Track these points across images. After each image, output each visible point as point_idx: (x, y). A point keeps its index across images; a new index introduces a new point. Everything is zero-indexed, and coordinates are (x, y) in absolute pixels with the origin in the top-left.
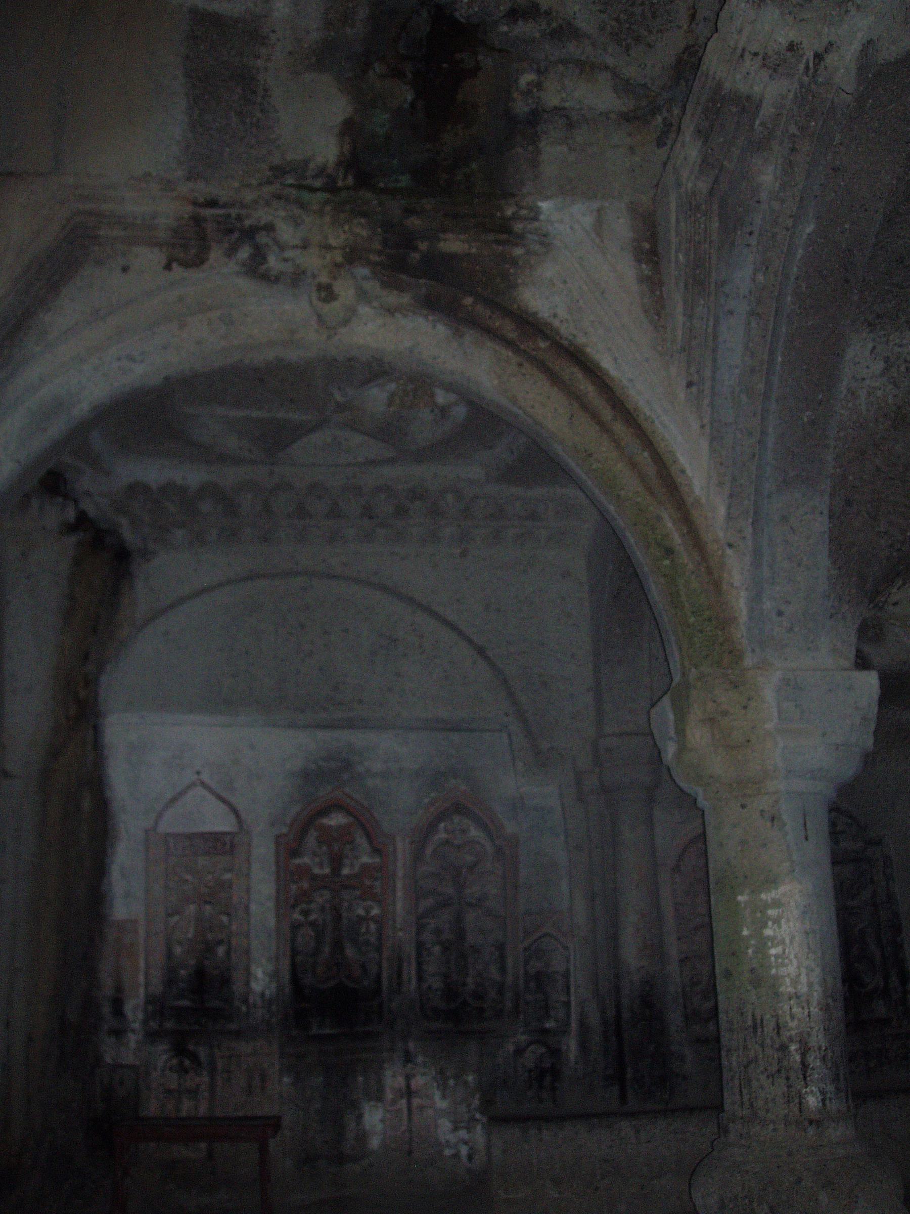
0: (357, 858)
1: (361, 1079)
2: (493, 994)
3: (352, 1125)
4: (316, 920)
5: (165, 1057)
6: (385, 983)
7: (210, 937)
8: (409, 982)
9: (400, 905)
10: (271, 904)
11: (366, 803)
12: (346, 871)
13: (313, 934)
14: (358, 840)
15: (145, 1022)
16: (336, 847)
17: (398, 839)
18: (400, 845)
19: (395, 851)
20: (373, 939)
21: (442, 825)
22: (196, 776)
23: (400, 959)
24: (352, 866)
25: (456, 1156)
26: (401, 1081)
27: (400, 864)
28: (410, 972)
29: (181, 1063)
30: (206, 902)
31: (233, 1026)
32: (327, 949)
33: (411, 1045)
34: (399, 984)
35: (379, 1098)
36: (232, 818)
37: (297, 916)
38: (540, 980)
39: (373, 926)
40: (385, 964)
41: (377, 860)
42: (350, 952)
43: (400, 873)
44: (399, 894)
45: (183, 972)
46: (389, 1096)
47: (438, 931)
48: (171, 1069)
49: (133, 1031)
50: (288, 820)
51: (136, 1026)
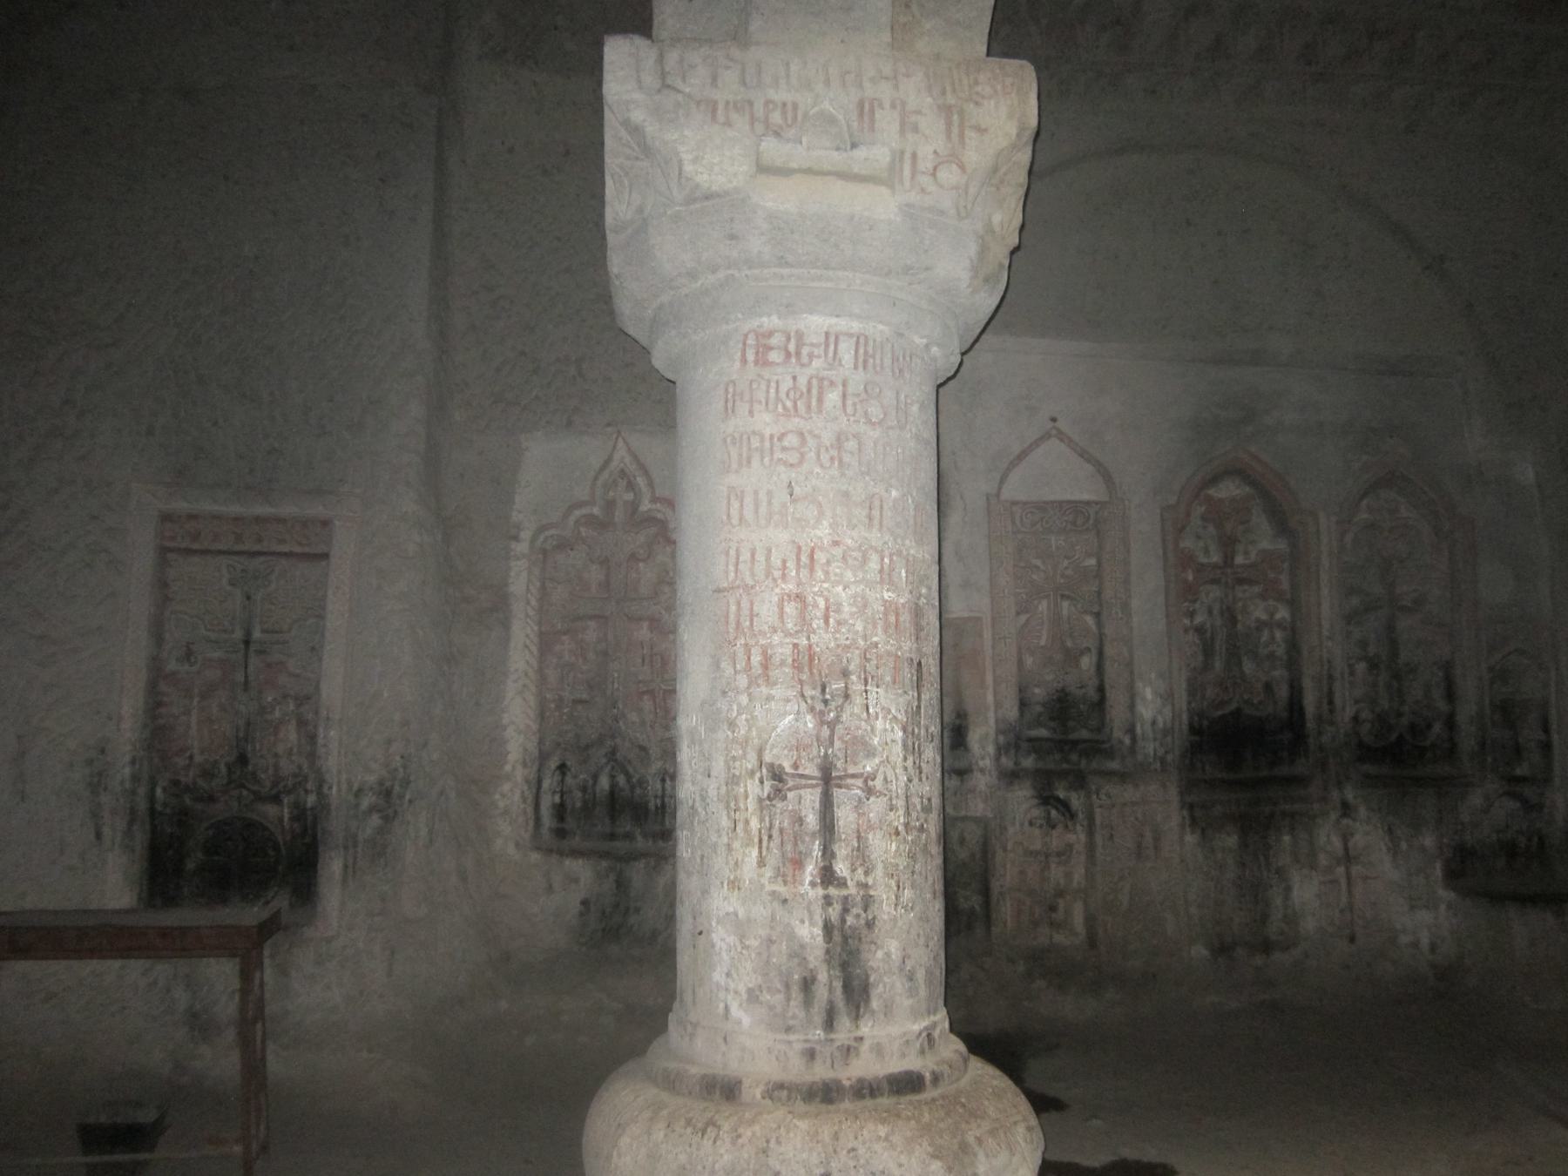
1: (1287, 838)
2: (1437, 728)
3: (1279, 901)
5: (1025, 806)
7: (1069, 644)
9: (1326, 605)
10: (1161, 599)
12: (1239, 560)
15: (998, 759)
20: (1280, 651)
21: (1365, 502)
22: (1051, 424)
23: (1331, 677)
24: (1246, 553)
25: (1415, 945)
26: (1337, 842)
29: (1048, 818)
30: (1063, 596)
31: (1114, 765)
32: (1218, 665)
33: (1350, 794)
34: (1331, 711)
35: (1313, 867)
38: (1507, 712)
39: (1278, 635)
40: (1307, 684)
41: (1282, 545)
42: (1248, 667)
43: (1325, 561)
44: (1325, 591)
45: (1037, 691)
46: (1323, 860)
47: (1363, 644)
48: (1031, 824)
49: (982, 771)
51: (987, 763)
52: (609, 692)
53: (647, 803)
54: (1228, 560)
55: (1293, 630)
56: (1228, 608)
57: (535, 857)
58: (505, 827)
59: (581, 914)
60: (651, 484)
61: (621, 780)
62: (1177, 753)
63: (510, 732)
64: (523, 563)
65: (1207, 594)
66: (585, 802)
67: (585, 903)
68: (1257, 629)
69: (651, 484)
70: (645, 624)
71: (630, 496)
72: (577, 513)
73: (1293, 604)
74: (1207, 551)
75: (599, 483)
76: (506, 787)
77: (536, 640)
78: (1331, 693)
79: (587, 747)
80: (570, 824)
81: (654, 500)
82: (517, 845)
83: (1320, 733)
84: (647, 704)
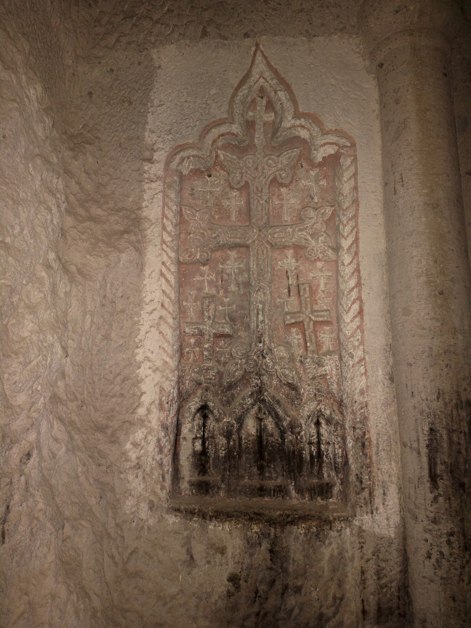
52: (253, 326)
53: (303, 449)
57: (172, 520)
58: (136, 484)
59: (229, 594)
60: (293, 100)
61: (270, 424)
63: (144, 371)
64: (158, 186)
66: (230, 451)
67: (233, 579)
69: (293, 100)
70: (290, 253)
71: (270, 117)
72: (215, 132)
75: (238, 99)
76: (139, 434)
77: (173, 268)
79: (230, 387)
80: (213, 476)
81: (297, 115)
82: (152, 506)
84: (295, 337)
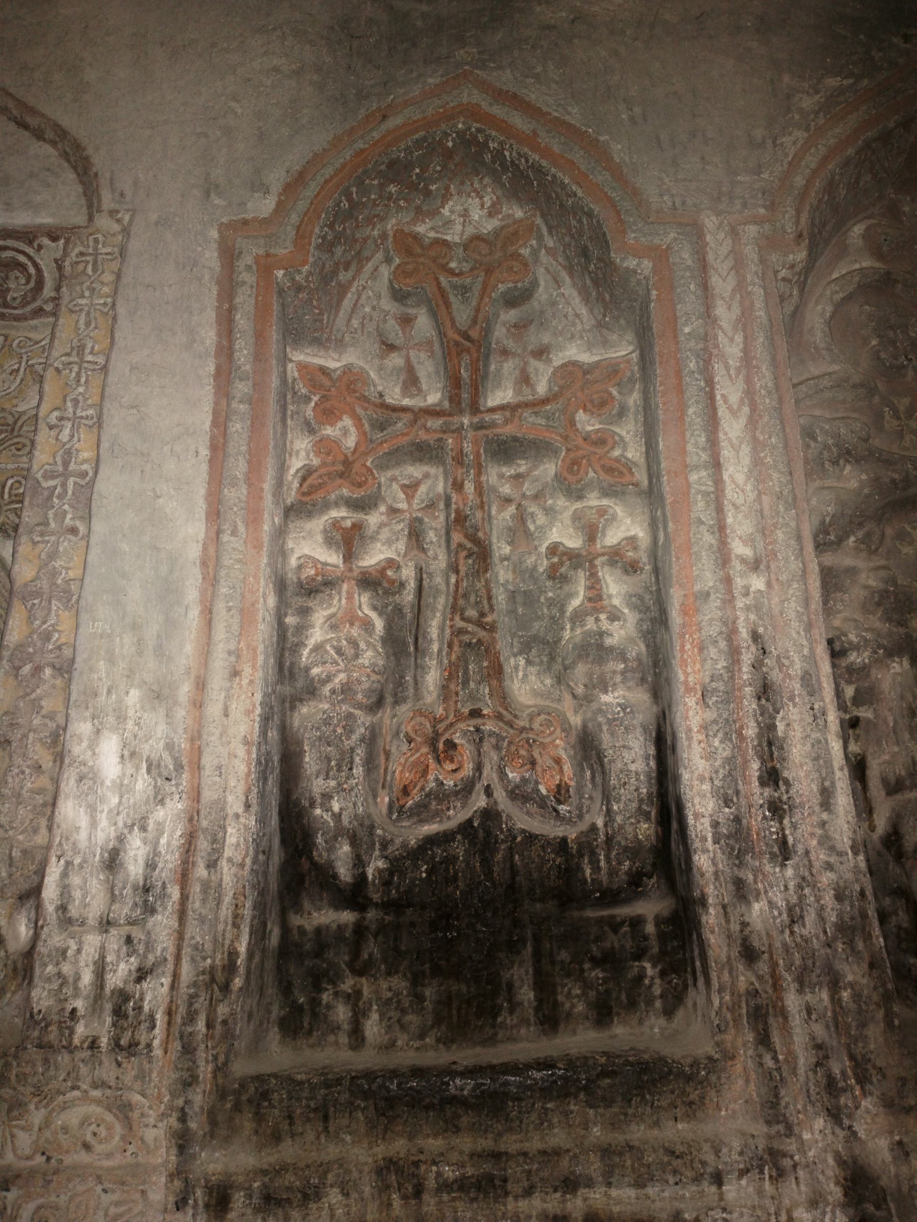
0: (541, 353)
4: (390, 563)
6: (701, 807)
8: (826, 796)
11: (574, 115)
12: (500, 395)
13: (379, 624)
14: (542, 294)
16: (462, 314)
17: (710, 222)
18: (718, 245)
19: (703, 266)
20: (622, 632)
23: (765, 691)
27: (726, 315)
28: (812, 744)
32: (432, 678)
36: (68, 187)
37: (310, 548)
39: (615, 588)
40: (691, 716)
42: (526, 685)
44: (733, 428)
50: (276, 178)
54: (465, 391)
55: (656, 571)
56: (461, 519)
62: (186, 970)
65: (410, 489)
68: (553, 573)
73: (652, 495)
74: (411, 382)
78: (770, 745)
83: (742, 892)
